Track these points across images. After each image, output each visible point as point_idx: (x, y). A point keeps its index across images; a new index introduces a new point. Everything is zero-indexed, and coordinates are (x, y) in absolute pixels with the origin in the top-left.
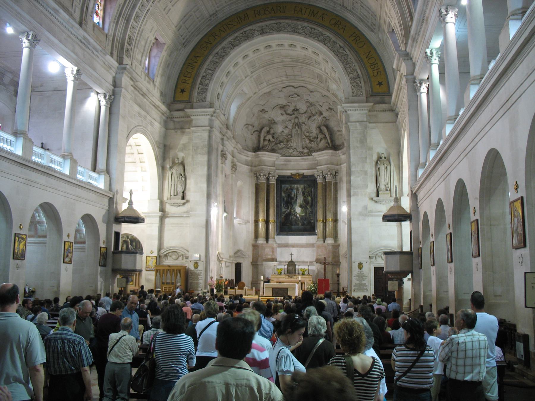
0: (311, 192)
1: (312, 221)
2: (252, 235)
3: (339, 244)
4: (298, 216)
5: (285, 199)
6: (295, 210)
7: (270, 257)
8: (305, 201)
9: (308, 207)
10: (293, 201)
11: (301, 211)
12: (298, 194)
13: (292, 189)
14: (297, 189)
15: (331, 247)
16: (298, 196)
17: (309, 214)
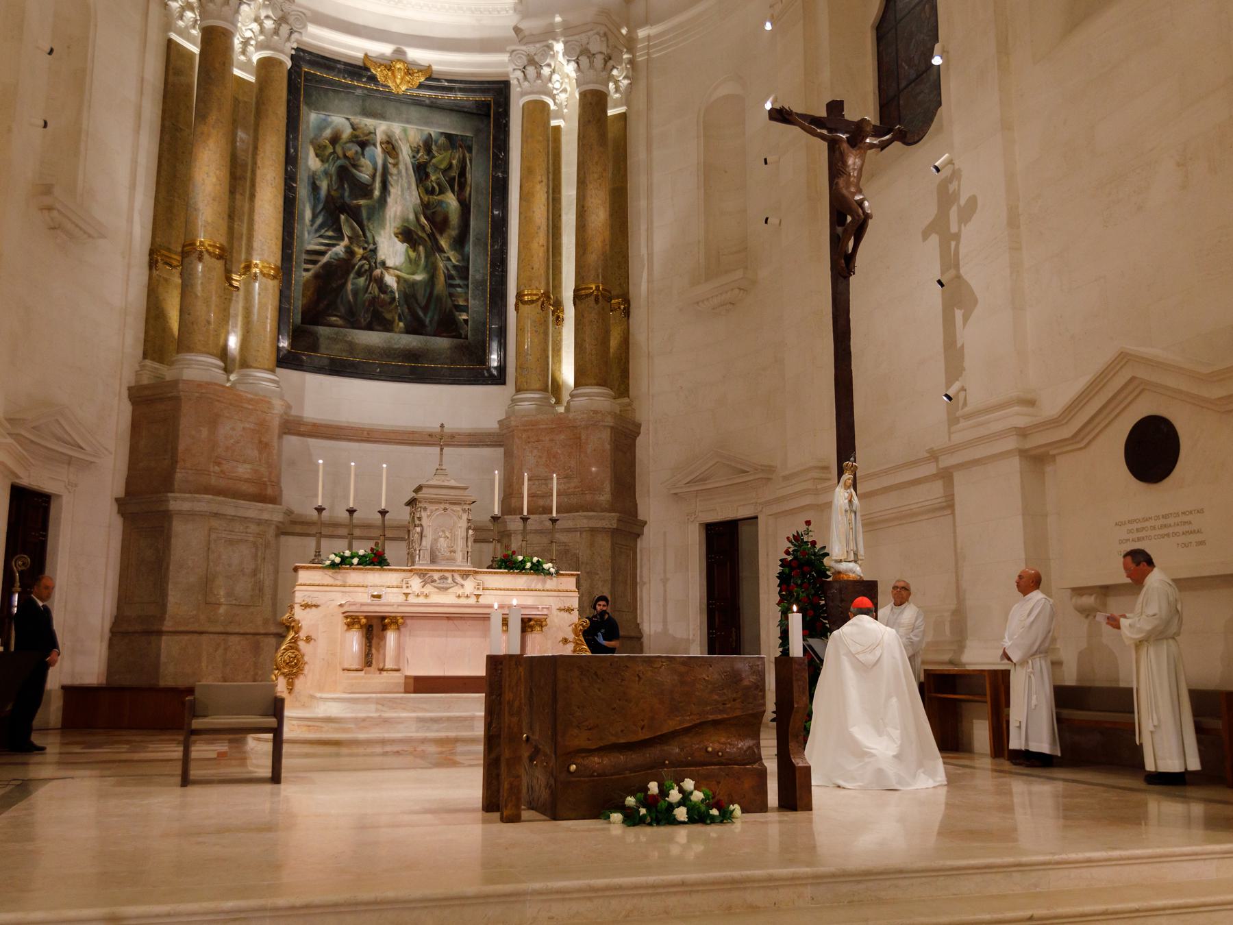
0: (462, 173)
1: (464, 317)
2: (131, 338)
3: (639, 426)
4: (390, 280)
5: (324, 185)
6: (374, 251)
7: (243, 470)
8: (426, 206)
9: (443, 243)
10: (362, 202)
11: (410, 260)
12: (393, 171)
13: (363, 143)
14: (391, 148)
15: (606, 435)
16: (392, 180)
17: (450, 277)
